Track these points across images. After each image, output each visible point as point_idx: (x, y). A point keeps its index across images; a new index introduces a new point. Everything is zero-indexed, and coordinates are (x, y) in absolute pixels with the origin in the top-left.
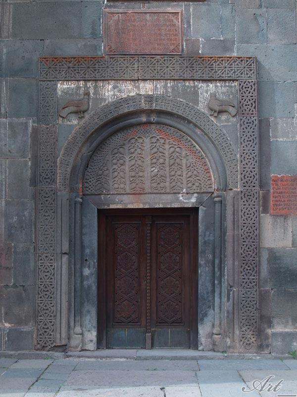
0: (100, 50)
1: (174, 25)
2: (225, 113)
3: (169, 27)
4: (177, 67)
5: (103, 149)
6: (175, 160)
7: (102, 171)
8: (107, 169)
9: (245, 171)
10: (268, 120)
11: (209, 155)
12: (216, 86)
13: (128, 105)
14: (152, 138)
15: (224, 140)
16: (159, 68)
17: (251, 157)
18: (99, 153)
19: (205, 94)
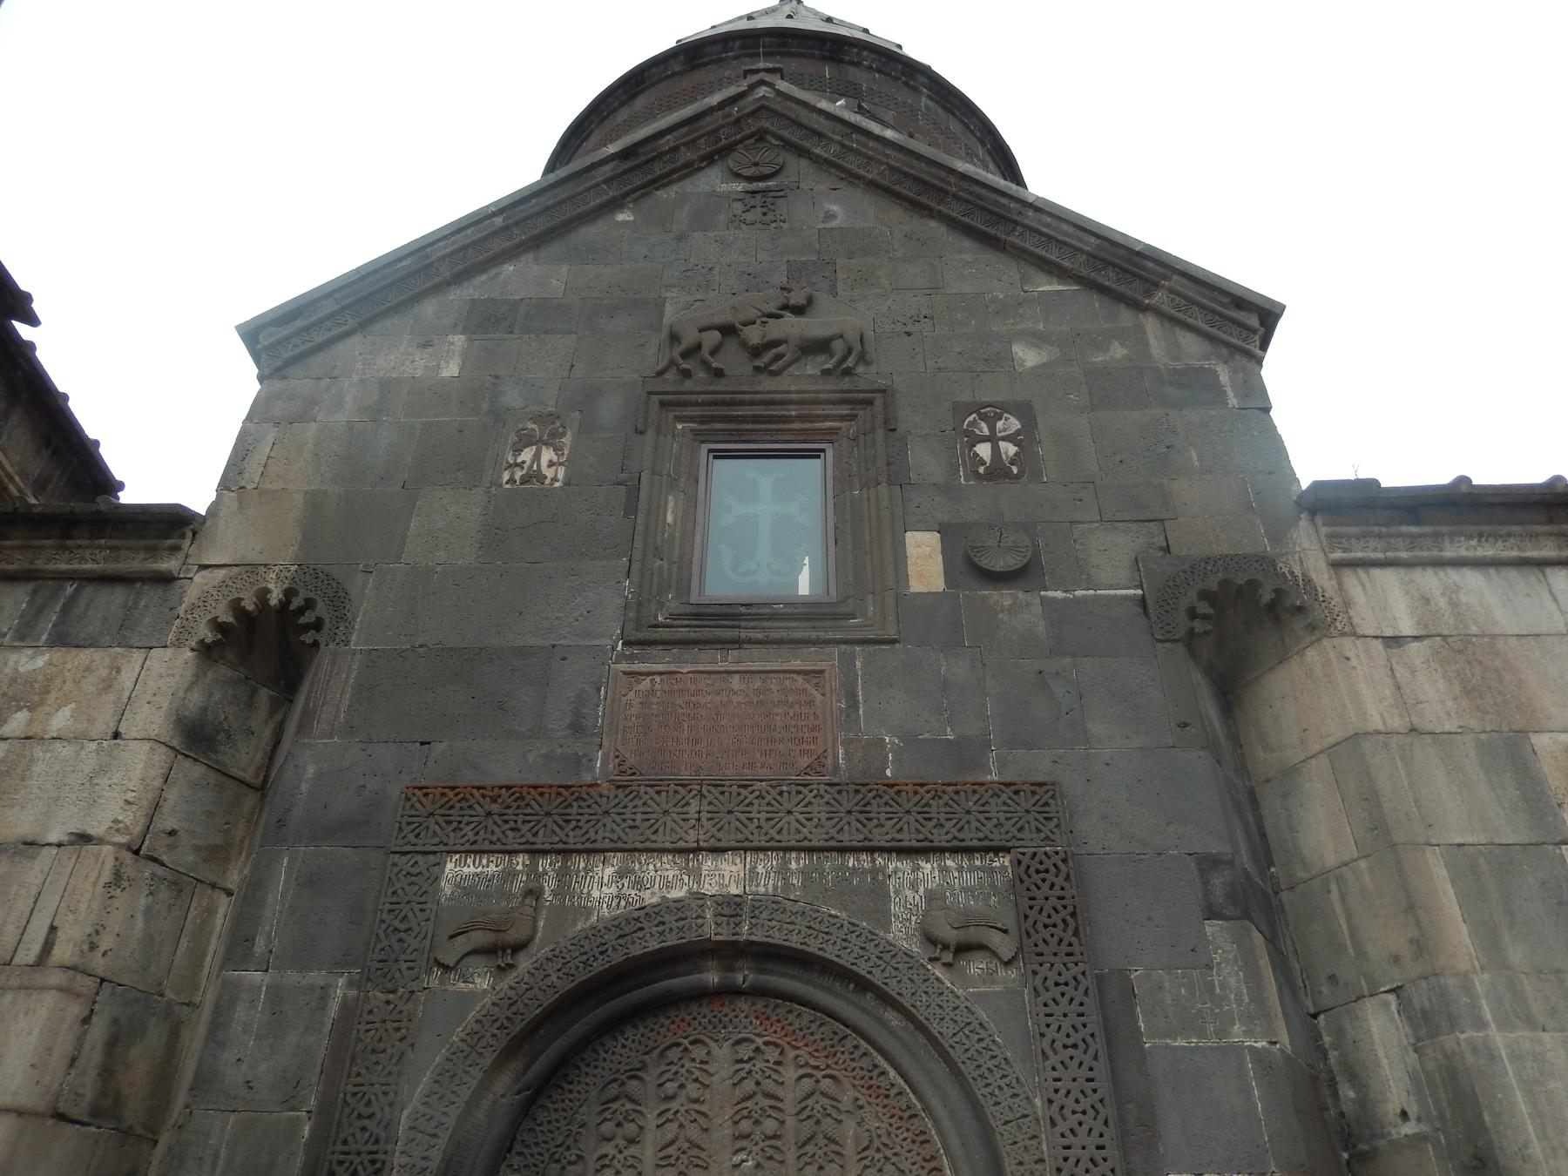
0: (592, 769)
1: (811, 702)
2: (978, 955)
3: (797, 707)
4: (819, 810)
5: (571, 1083)
6: (818, 1122)
7: (558, 1166)
8: (580, 1157)
9: (1072, 1161)
10: (1123, 974)
11: (936, 1103)
12: (944, 870)
13: (660, 929)
14: (738, 1042)
15: (983, 1044)
16: (763, 816)
17: (1085, 1104)
18: (556, 1096)
19: (910, 894)
